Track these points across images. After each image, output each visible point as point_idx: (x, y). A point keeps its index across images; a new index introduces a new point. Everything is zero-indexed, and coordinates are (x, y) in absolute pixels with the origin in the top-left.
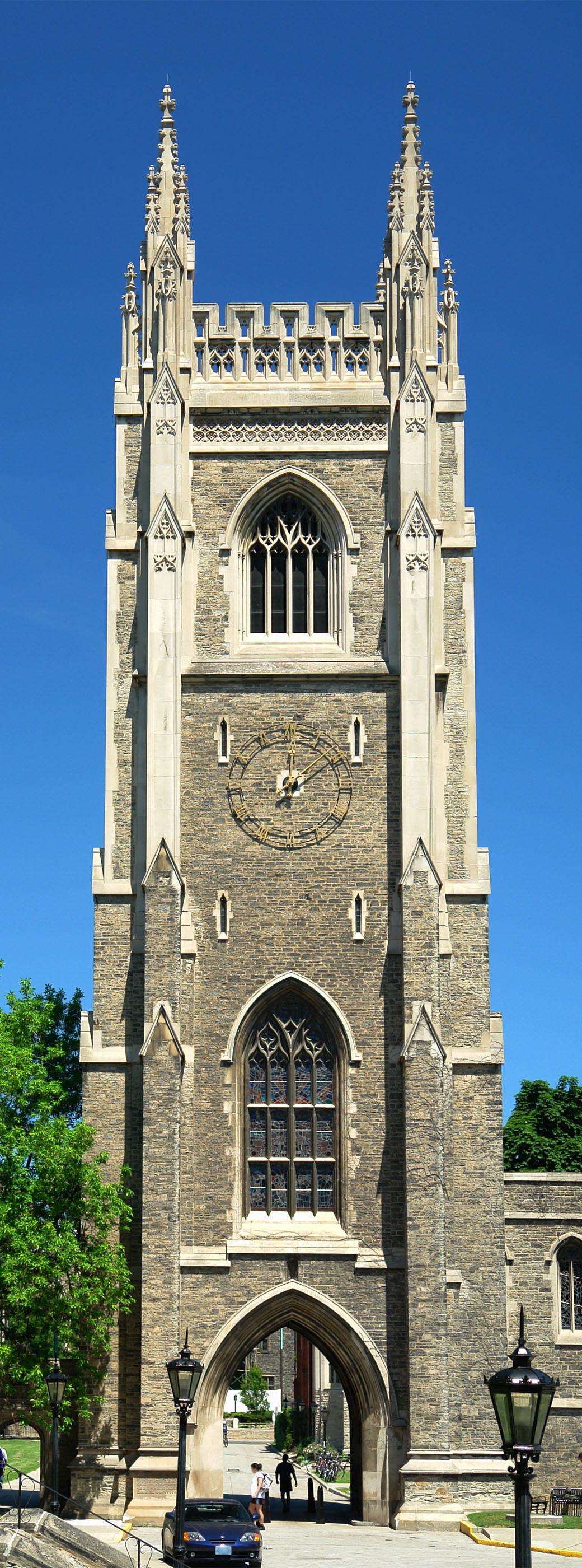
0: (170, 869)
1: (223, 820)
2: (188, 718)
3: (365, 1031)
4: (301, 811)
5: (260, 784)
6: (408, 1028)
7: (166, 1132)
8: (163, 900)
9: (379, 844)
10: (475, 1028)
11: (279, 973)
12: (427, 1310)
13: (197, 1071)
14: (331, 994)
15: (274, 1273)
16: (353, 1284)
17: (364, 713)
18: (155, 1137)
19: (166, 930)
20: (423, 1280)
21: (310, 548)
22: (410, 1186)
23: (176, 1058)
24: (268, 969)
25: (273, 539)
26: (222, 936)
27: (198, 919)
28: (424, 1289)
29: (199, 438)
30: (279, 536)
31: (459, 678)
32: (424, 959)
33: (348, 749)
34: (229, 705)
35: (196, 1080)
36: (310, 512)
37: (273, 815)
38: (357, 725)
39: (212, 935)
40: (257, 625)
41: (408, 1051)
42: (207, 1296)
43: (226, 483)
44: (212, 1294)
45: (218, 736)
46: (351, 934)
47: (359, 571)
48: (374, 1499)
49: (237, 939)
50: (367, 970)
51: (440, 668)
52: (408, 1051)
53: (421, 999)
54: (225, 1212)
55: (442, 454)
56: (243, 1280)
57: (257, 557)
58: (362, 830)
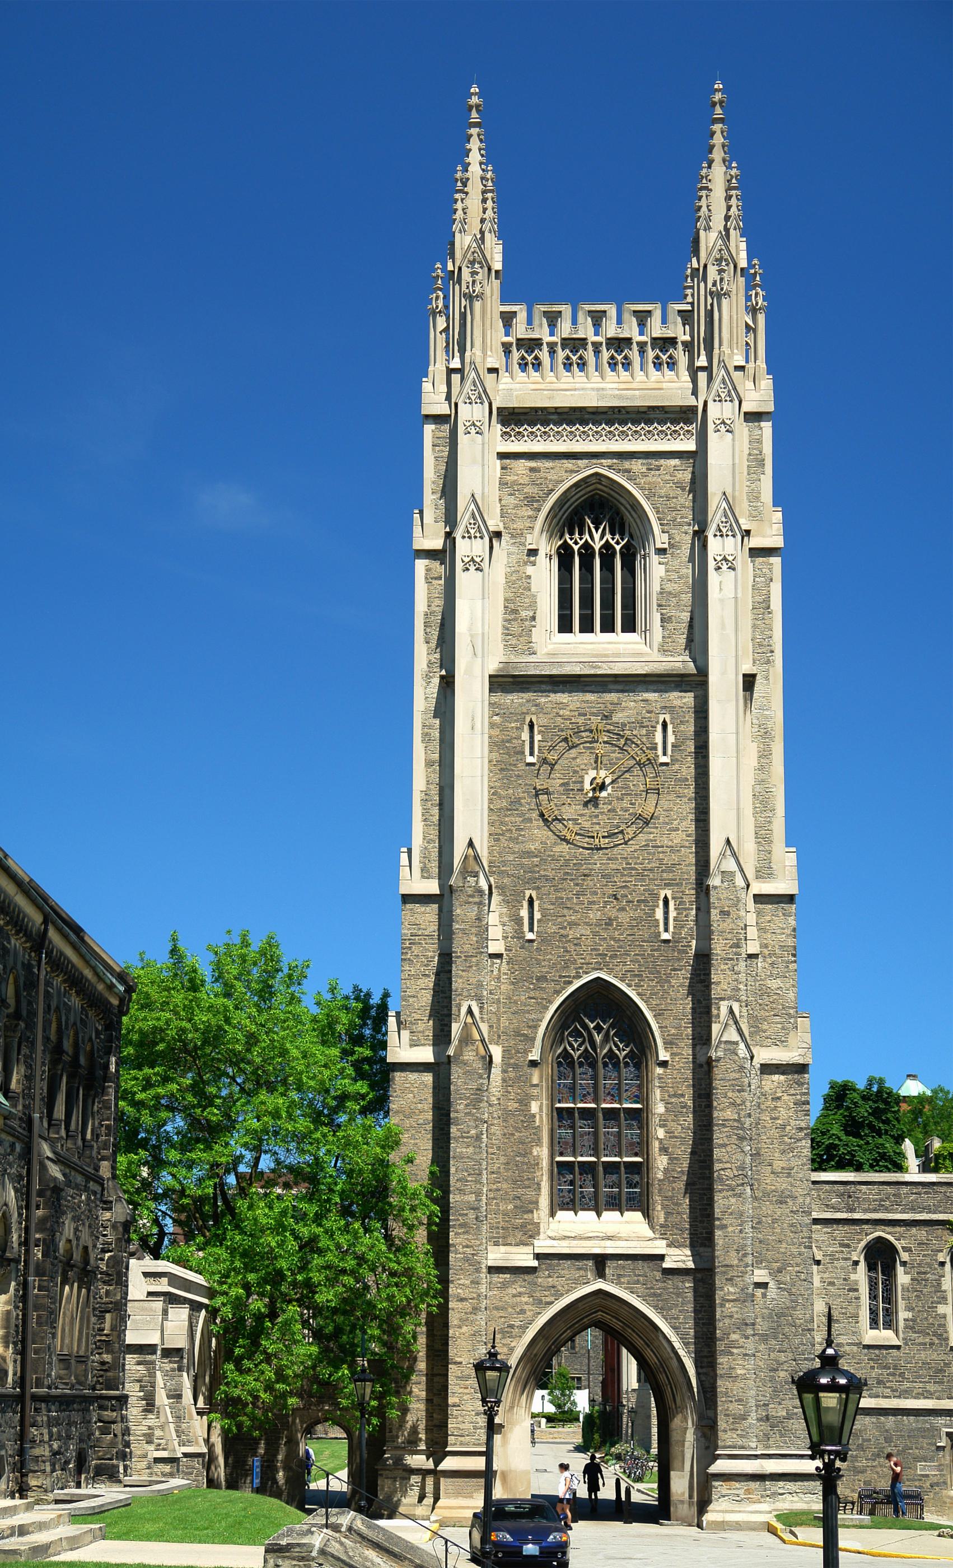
0: (477, 869)
1: (530, 820)
2: (495, 718)
3: (673, 1031)
4: (609, 811)
5: (567, 784)
6: (715, 1028)
7: (473, 1132)
8: (471, 900)
9: (687, 844)
11: (587, 973)
12: (734, 1309)
13: (504, 1071)
14: (639, 994)
15: (582, 1273)
16: (660, 1285)
17: (671, 713)
18: (463, 1137)
19: (473, 930)
20: (730, 1280)
21: (618, 548)
22: (717, 1186)
23: (484, 1057)
24: (576, 969)
25: (581, 539)
26: (530, 936)
27: (506, 919)
28: (731, 1289)
29: (506, 438)
30: (587, 536)
31: (767, 678)
32: (732, 959)
33: (656, 749)
34: (536, 705)
35: (504, 1080)
36: (618, 512)
37: (581, 815)
38: (665, 725)
39: (519, 935)
40: (565, 625)
41: (716, 1051)
42: (514, 1296)
43: (533, 483)
44: (520, 1294)
45: (525, 736)
46: (659, 934)
47: (667, 571)
48: (681, 1498)
49: (545, 939)
50: (675, 970)
51: (747, 668)
52: (716, 1051)
53: (729, 999)
54: (532, 1212)
55: (750, 454)
56: (550, 1279)
57: (565, 557)
58: (670, 830)
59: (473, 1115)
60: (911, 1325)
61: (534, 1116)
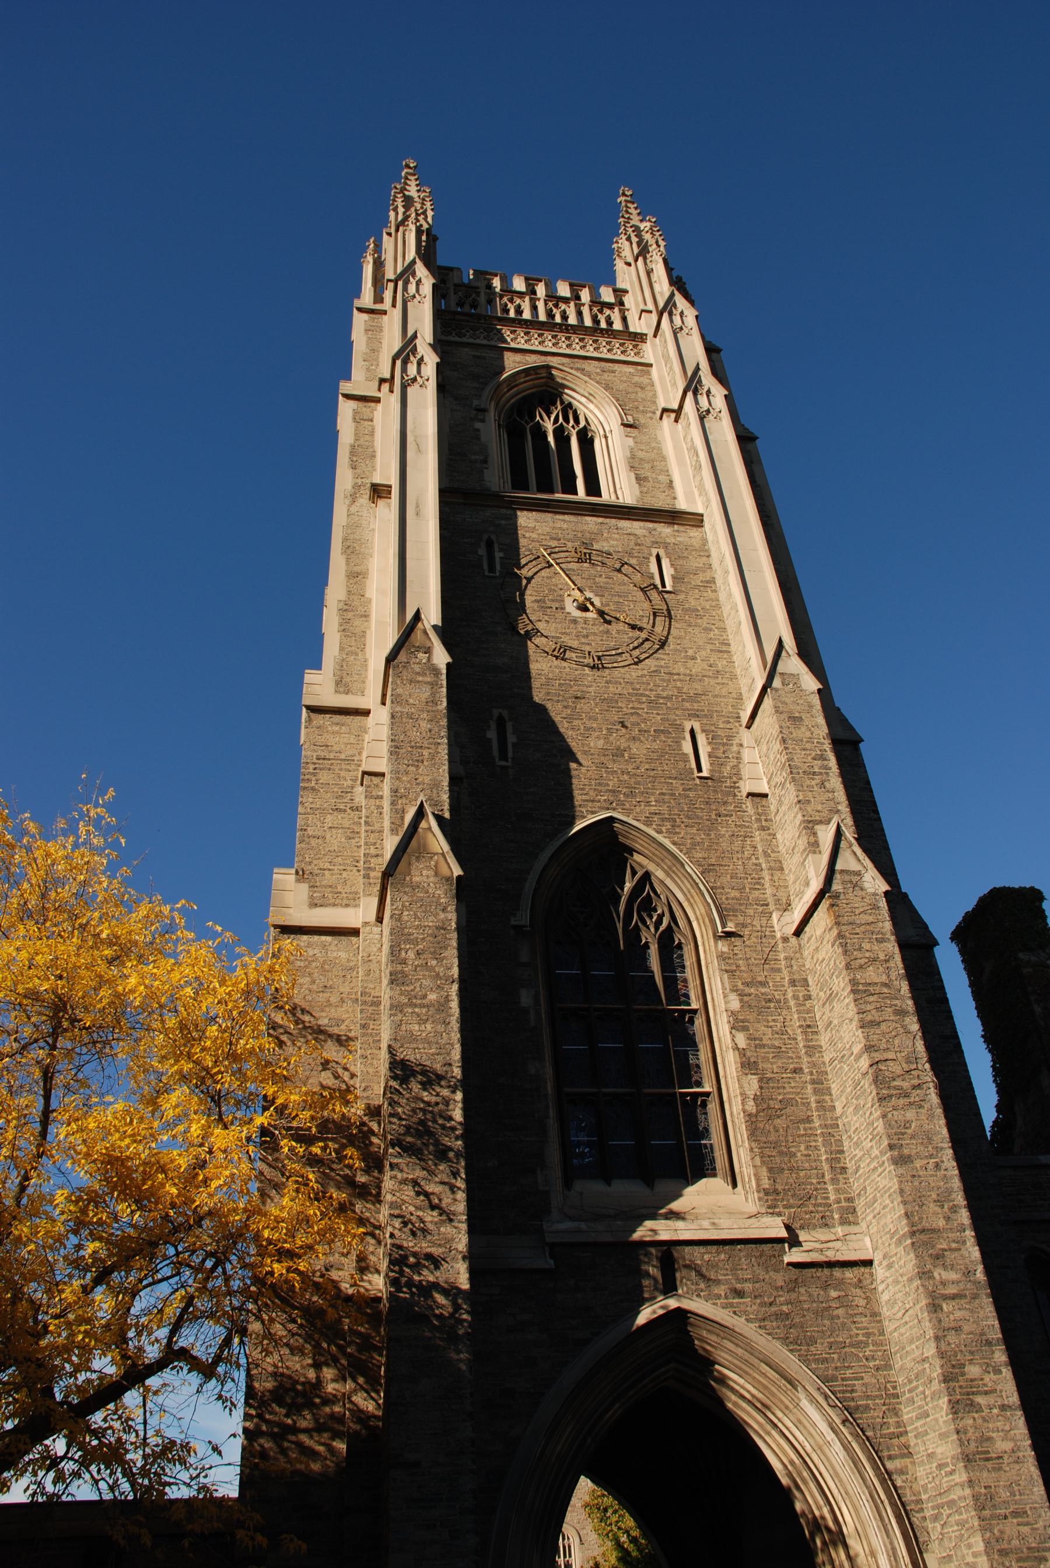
0: (428, 644)
7: (432, 997)
8: (420, 679)
11: (593, 813)
36: (570, 405)
45: (482, 551)
59: (432, 969)
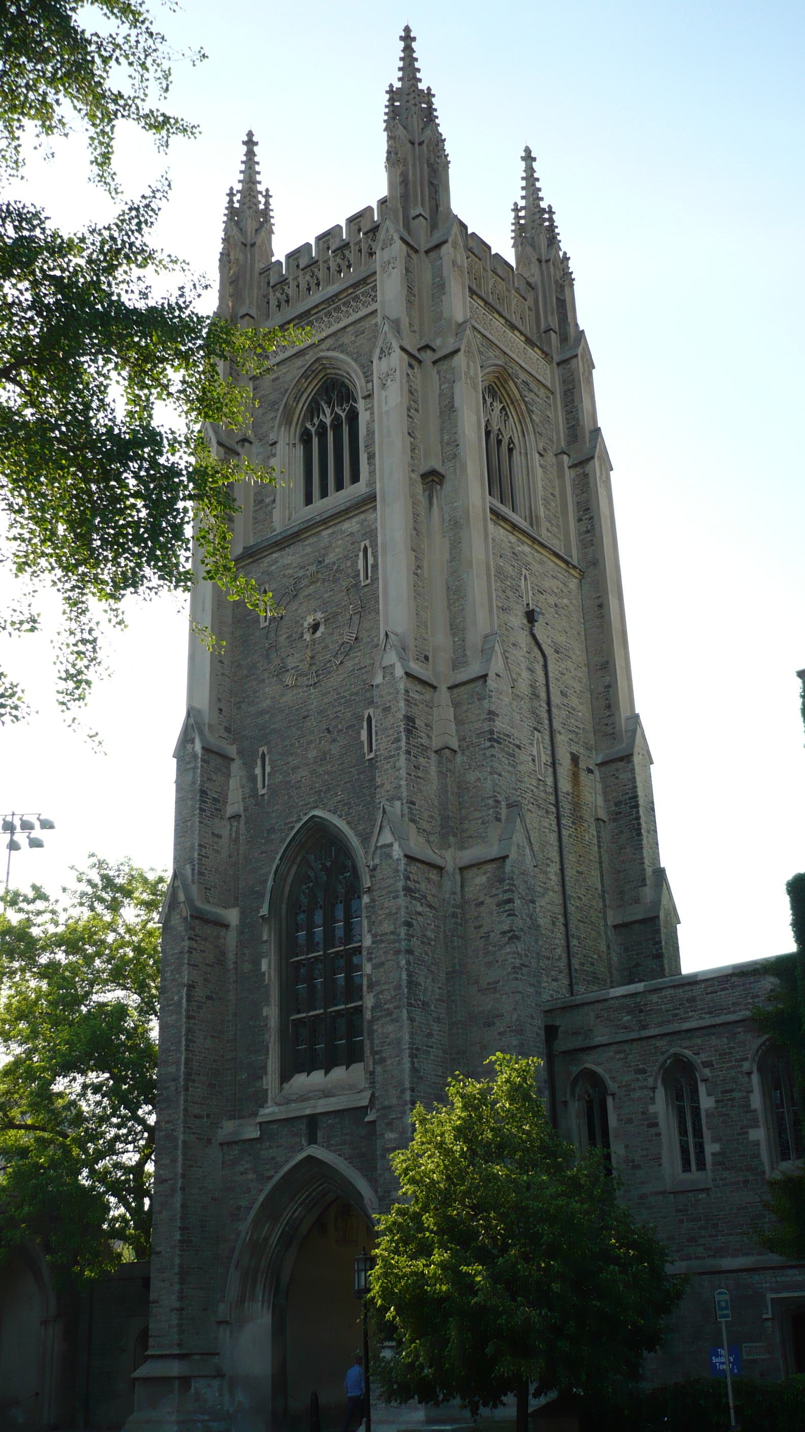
10: (483, 823)
13: (241, 933)
26: (262, 792)
33: (358, 575)
41: (373, 859)
42: (242, 1174)
57: (306, 439)
60: (721, 1161)
61: (264, 974)
